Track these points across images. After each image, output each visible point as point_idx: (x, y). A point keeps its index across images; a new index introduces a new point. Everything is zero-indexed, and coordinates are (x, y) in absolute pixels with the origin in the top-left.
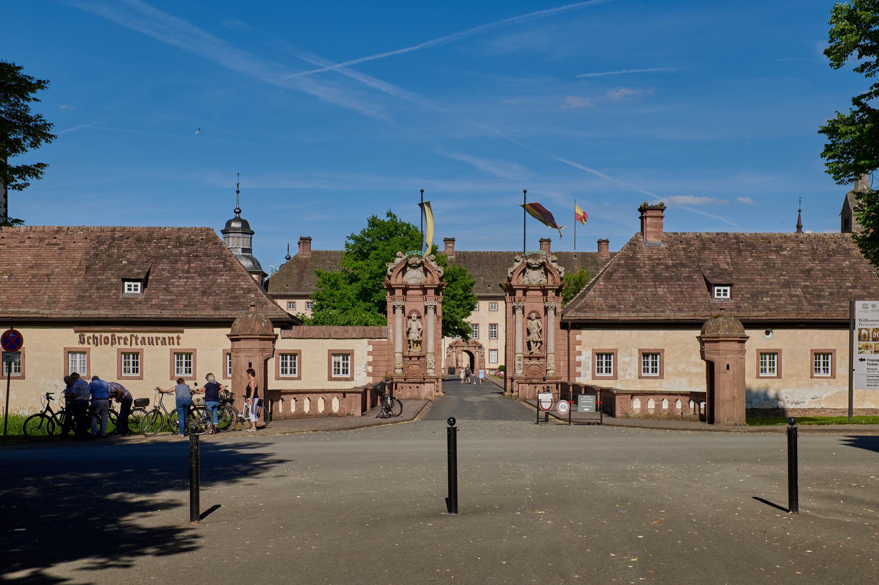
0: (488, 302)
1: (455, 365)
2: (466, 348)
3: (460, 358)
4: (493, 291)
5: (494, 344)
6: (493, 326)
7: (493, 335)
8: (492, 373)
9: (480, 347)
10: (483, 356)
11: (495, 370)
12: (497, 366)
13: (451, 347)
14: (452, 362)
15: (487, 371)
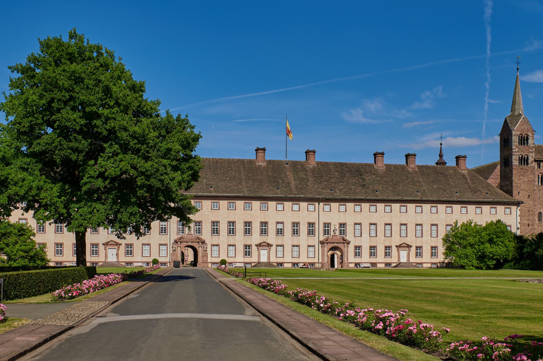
0: (210, 201)
1: (179, 259)
2: (190, 244)
3: (186, 254)
4: (215, 191)
5: (216, 240)
6: (215, 223)
7: (215, 231)
8: (215, 266)
9: (203, 242)
10: (206, 251)
11: (217, 263)
12: (218, 260)
13: (176, 242)
14: (177, 256)
15: (210, 265)
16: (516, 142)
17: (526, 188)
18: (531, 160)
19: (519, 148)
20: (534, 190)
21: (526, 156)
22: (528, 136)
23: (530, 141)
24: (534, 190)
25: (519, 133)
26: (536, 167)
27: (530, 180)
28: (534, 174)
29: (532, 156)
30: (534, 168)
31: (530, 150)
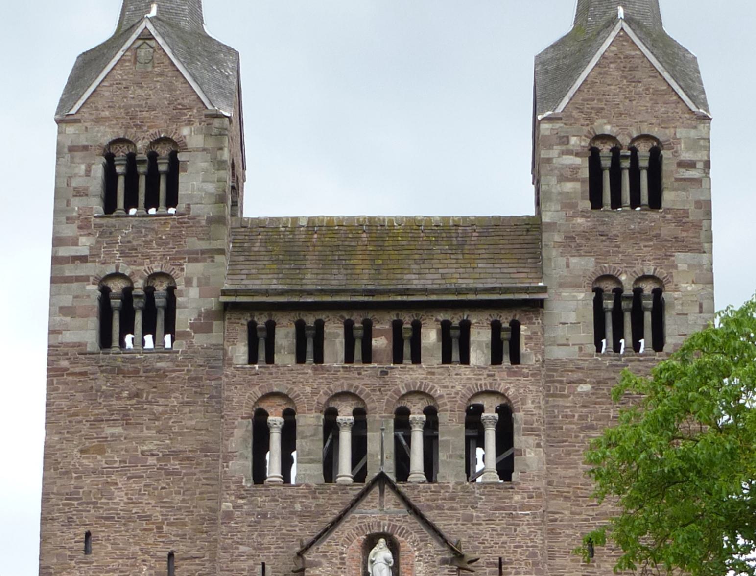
16: (81, 193)
17: (149, 506)
18: (191, 304)
19: (106, 233)
20: (212, 519)
21: (161, 288)
22: (176, 147)
23: (196, 184)
24: (212, 519)
25: (105, 135)
26: (240, 352)
27: (185, 445)
28: (217, 403)
29: (204, 283)
30: (217, 359)
31: (195, 243)
